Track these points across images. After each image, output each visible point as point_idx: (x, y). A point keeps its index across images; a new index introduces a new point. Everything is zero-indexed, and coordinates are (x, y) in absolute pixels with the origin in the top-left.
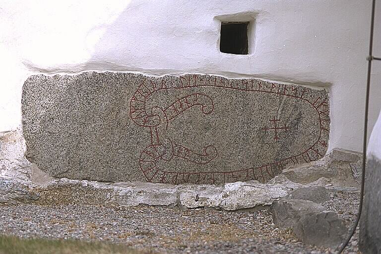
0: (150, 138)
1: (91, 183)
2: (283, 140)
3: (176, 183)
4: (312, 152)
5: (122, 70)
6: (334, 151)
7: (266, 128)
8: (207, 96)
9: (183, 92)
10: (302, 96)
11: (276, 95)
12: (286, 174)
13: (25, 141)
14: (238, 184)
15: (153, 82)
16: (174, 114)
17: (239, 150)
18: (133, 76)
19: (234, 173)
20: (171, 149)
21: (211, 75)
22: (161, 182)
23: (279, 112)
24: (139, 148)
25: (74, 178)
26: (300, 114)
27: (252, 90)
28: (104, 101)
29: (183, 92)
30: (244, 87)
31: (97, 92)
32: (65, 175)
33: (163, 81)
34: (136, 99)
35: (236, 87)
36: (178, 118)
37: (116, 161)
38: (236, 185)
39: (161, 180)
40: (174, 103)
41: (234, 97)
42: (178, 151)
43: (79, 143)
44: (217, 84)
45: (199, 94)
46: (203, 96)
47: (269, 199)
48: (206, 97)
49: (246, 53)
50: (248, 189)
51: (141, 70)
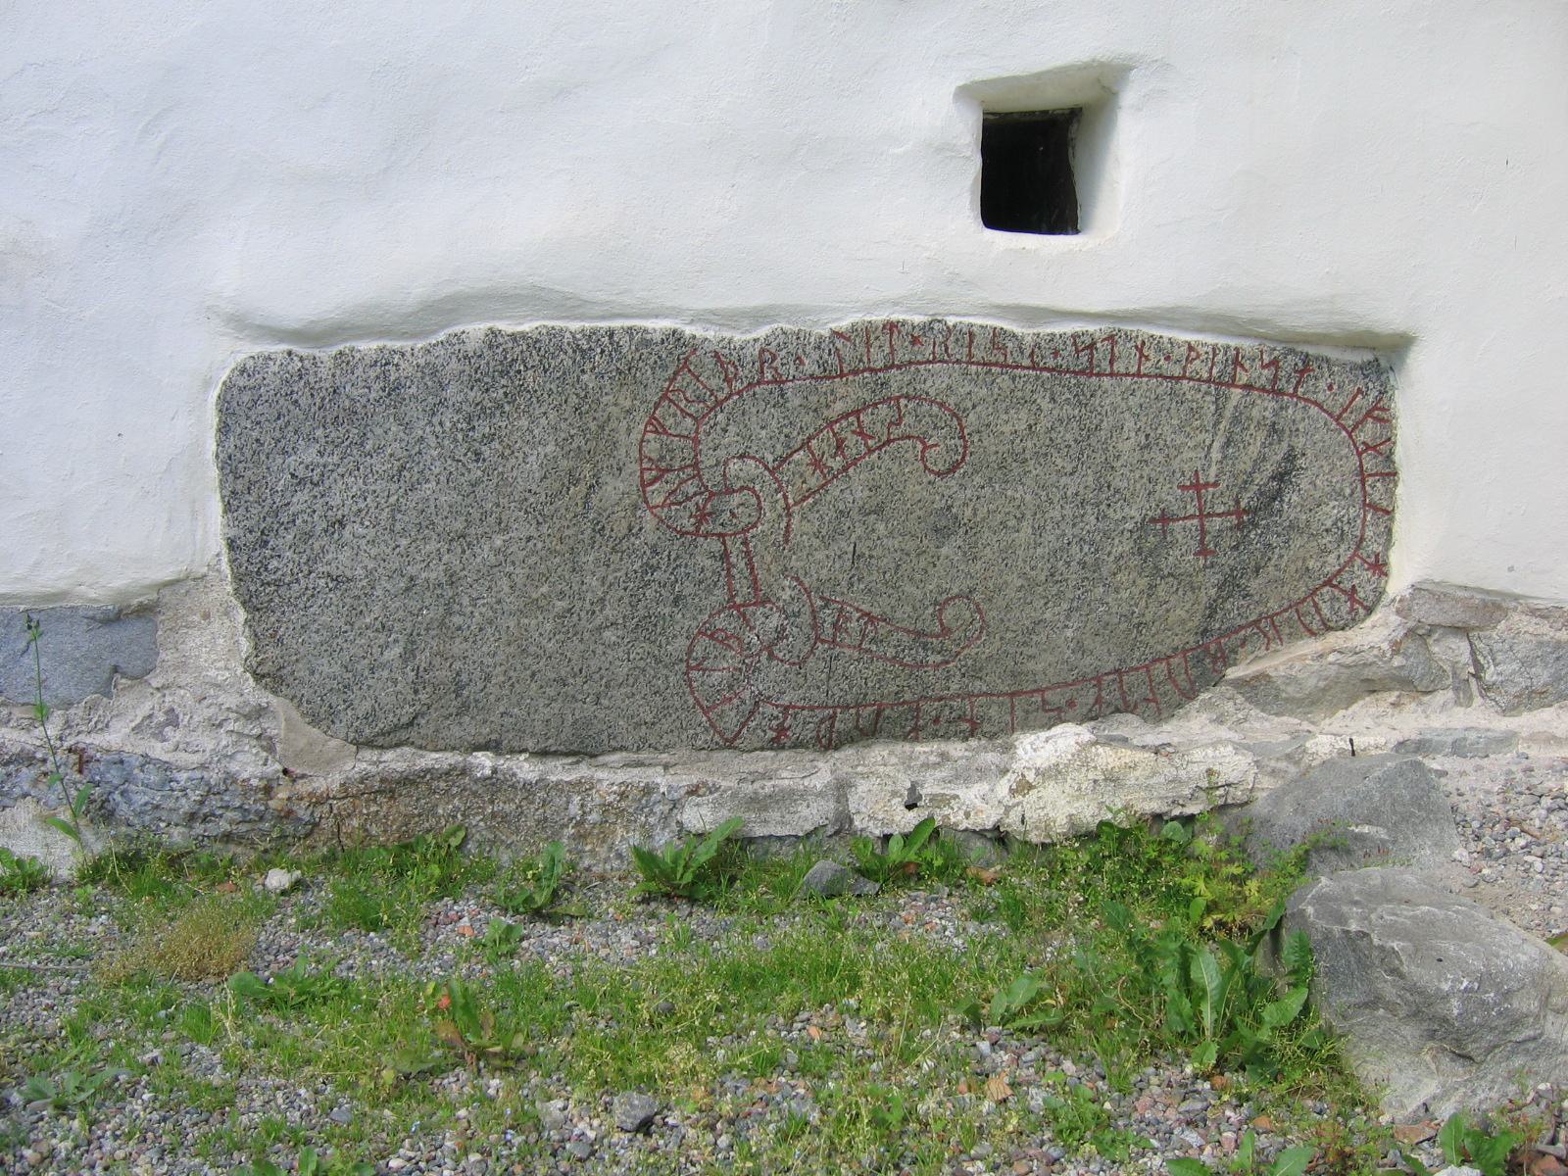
0: (723, 581)
1: (504, 763)
2: (1227, 560)
3: (829, 742)
4: (1334, 599)
5: (603, 318)
6: (1416, 589)
7: (1165, 518)
8: (942, 405)
9: (848, 394)
10: (1296, 389)
11: (1204, 387)
12: (1240, 684)
13: (242, 611)
14: (1066, 738)
15: (724, 360)
16: (813, 482)
17: (1065, 606)
18: (645, 342)
19: (1048, 695)
20: (806, 618)
21: (951, 321)
22: (776, 745)
23: (1216, 455)
24: (685, 622)
25: (441, 744)
26: (1290, 457)
27: (1111, 375)
28: (535, 450)
29: (848, 394)
30: (1082, 363)
31: (507, 408)
32: (403, 735)
33: (766, 356)
34: (660, 429)
35: (1051, 363)
36: (828, 498)
37: (596, 677)
38: (1062, 744)
39: (773, 740)
40: (810, 439)
41: (1046, 405)
42: (835, 625)
43: (449, 613)
44: (979, 354)
45: (907, 397)
46: (926, 407)
47: (1187, 792)
48: (935, 408)
49: (1076, 231)
50: (1107, 757)
51: (674, 312)
